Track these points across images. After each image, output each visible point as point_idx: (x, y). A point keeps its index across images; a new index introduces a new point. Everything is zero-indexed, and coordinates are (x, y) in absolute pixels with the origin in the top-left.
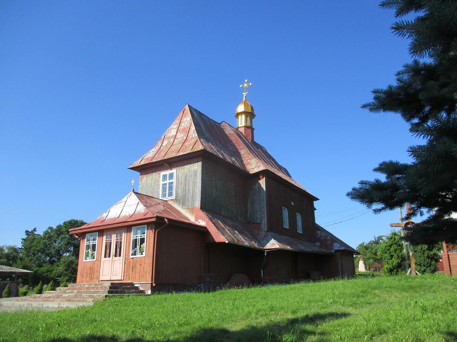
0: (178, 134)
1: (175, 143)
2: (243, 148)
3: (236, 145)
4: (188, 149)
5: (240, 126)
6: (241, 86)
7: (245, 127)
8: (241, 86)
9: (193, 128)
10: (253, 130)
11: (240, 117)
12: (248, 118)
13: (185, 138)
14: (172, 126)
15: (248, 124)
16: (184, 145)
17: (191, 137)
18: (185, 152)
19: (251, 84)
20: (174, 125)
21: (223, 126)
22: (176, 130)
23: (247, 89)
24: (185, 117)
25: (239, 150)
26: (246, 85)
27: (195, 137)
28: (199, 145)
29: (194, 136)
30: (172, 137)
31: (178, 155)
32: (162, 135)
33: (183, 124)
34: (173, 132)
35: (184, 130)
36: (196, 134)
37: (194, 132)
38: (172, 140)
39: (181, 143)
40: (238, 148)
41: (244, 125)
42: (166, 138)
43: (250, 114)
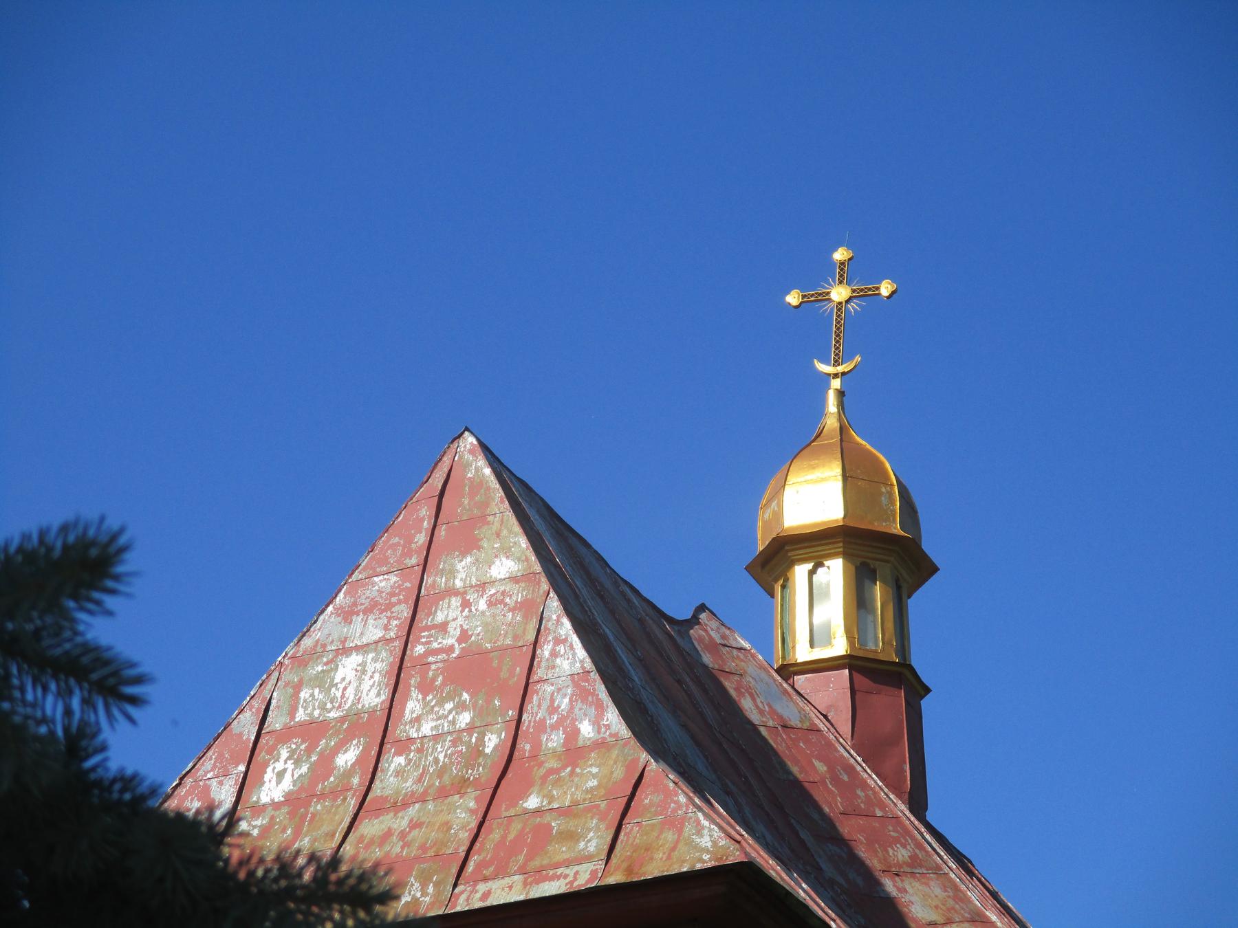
0: (413, 706)
1: (387, 784)
2: (914, 861)
3: (846, 828)
4: (561, 851)
5: (803, 653)
6: (793, 298)
7: (855, 663)
8: (793, 298)
9: (568, 655)
10: (917, 690)
11: (801, 572)
12: (878, 591)
13: (492, 741)
14: (327, 626)
15: (879, 643)
16: (502, 809)
17: (555, 740)
18: (539, 875)
19: (886, 289)
20: (347, 615)
21: (713, 647)
22: (379, 665)
23: (848, 333)
24: (469, 544)
25: (889, 885)
26: (839, 293)
27: (600, 745)
28: (675, 823)
29: (586, 729)
30: (353, 725)
31: (469, 899)
32: (235, 704)
33: (448, 611)
34: (358, 682)
35: (471, 669)
36: (612, 716)
37: (582, 694)
38: (347, 758)
39: (460, 786)
40: (875, 863)
41: (839, 647)
42: (286, 735)
43: (885, 555)
